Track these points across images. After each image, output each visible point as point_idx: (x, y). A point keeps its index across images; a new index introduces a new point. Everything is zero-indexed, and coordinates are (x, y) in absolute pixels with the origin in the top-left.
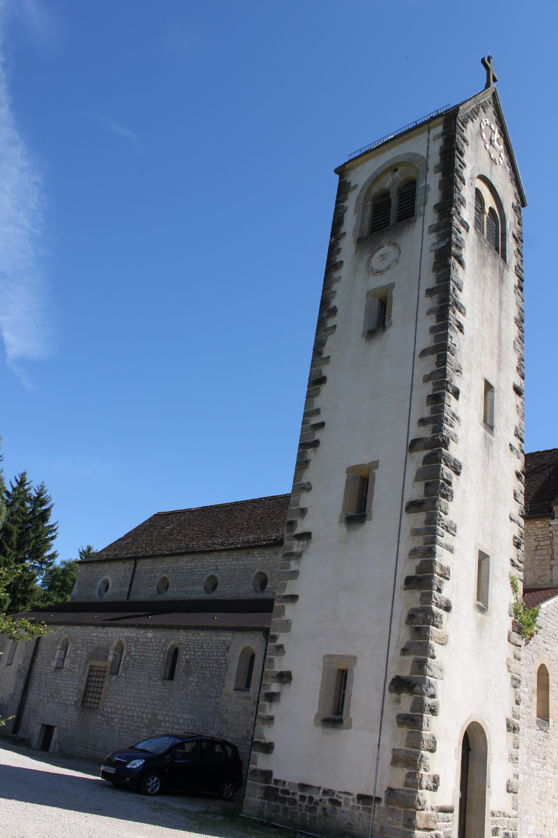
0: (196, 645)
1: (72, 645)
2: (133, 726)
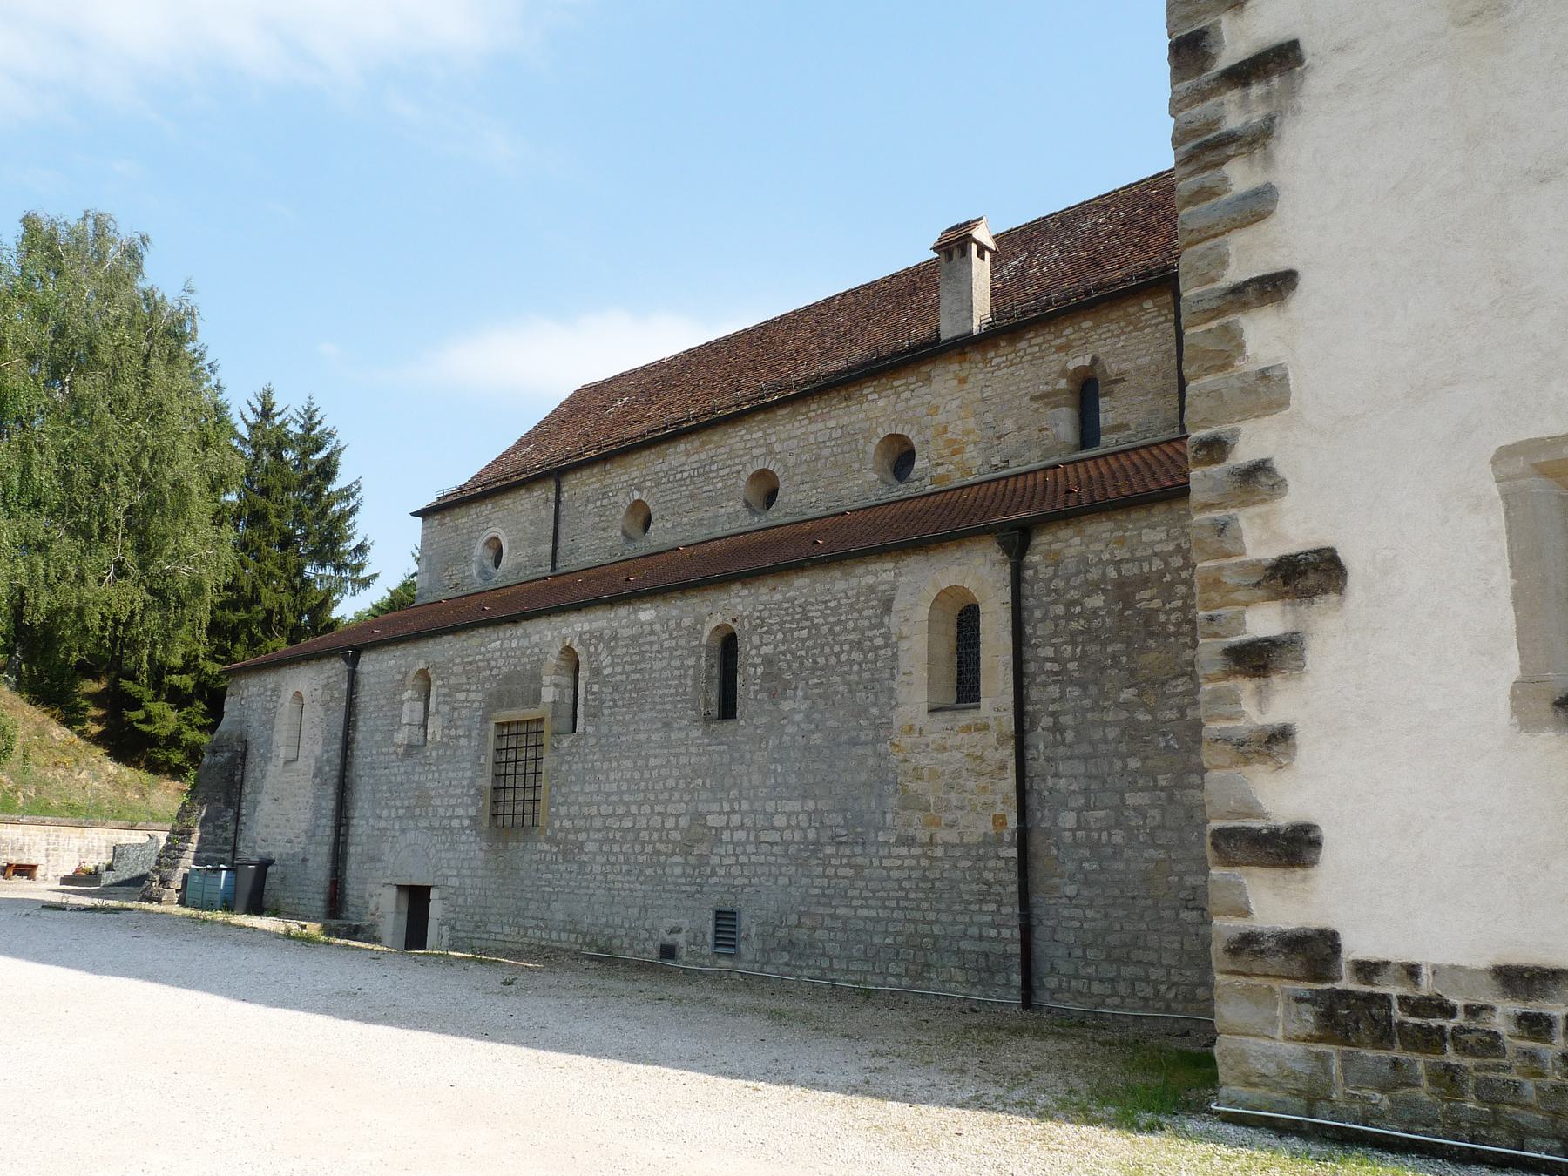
0: (787, 614)
1: (439, 683)
2: (642, 852)
